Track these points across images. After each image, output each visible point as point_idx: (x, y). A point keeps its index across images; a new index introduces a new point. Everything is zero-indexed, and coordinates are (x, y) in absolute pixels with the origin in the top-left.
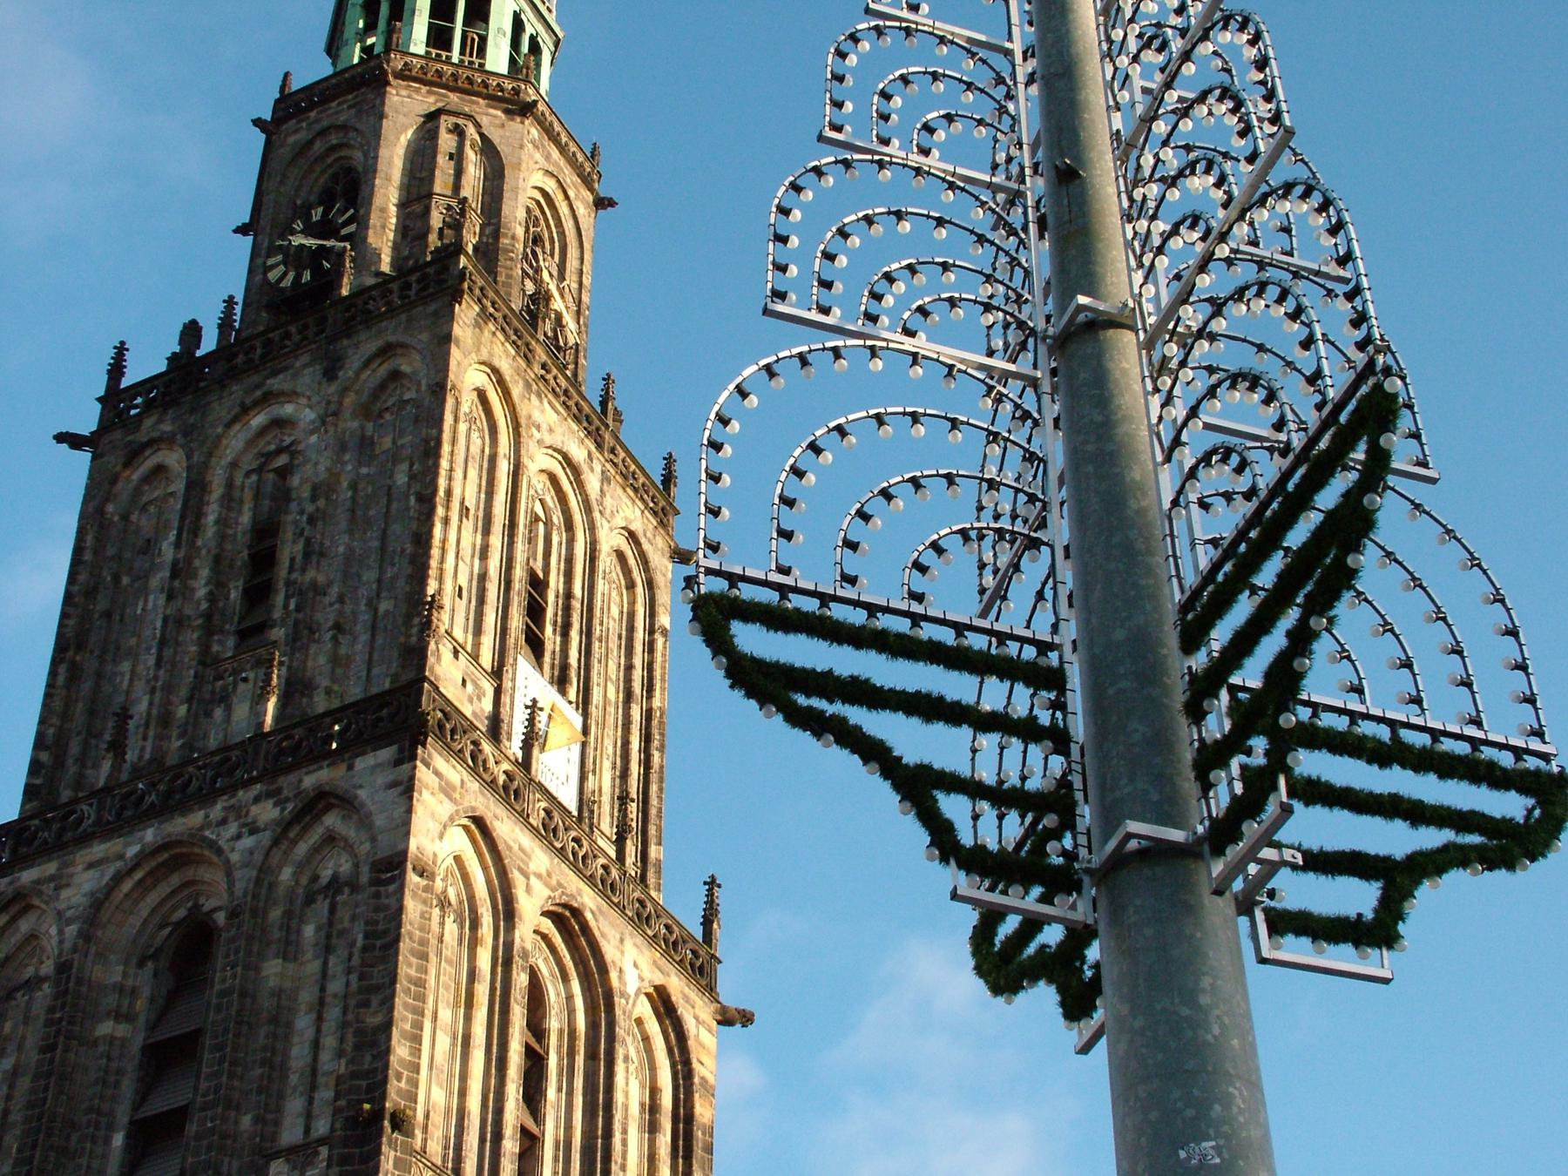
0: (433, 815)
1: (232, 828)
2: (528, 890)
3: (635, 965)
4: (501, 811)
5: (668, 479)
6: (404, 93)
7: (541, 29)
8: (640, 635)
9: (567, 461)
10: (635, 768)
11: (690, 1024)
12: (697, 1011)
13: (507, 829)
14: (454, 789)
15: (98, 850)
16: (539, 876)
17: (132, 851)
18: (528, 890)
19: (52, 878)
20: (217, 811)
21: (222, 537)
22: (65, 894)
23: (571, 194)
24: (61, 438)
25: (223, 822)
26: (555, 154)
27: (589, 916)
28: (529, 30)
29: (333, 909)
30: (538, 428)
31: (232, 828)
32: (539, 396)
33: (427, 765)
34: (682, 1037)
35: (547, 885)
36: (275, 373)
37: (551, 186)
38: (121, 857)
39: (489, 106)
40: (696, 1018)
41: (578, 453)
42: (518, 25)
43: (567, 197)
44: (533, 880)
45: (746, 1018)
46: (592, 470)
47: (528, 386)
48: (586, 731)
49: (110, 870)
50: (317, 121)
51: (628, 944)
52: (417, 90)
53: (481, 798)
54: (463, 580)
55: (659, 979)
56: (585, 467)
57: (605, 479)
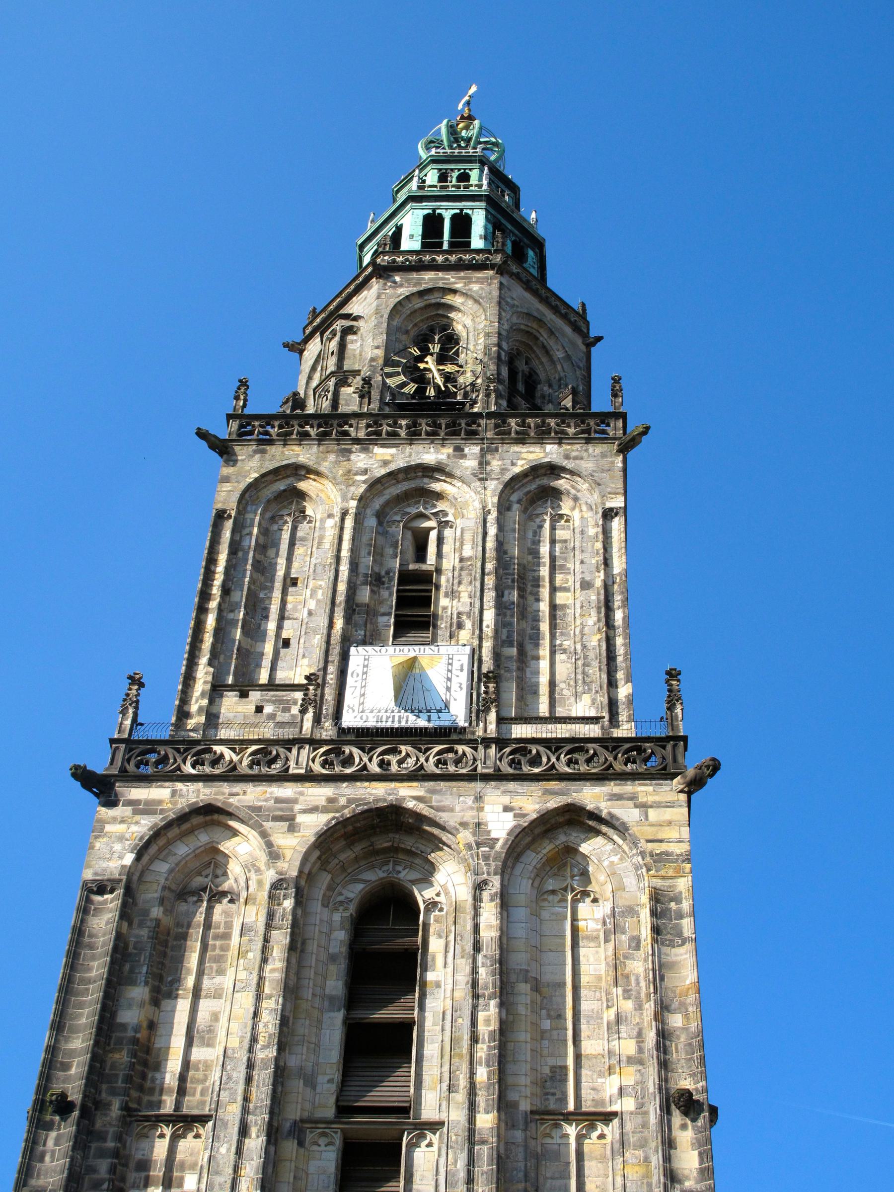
0: (121, 838)
2: (293, 828)
3: (507, 809)
12: (642, 799)
14: (160, 802)
16: (314, 810)
18: (293, 828)
23: (458, 286)
26: (428, 276)
27: (410, 804)
32: (365, 450)
35: (325, 810)
40: (644, 807)
44: (300, 819)
53: (207, 791)
55: (553, 803)
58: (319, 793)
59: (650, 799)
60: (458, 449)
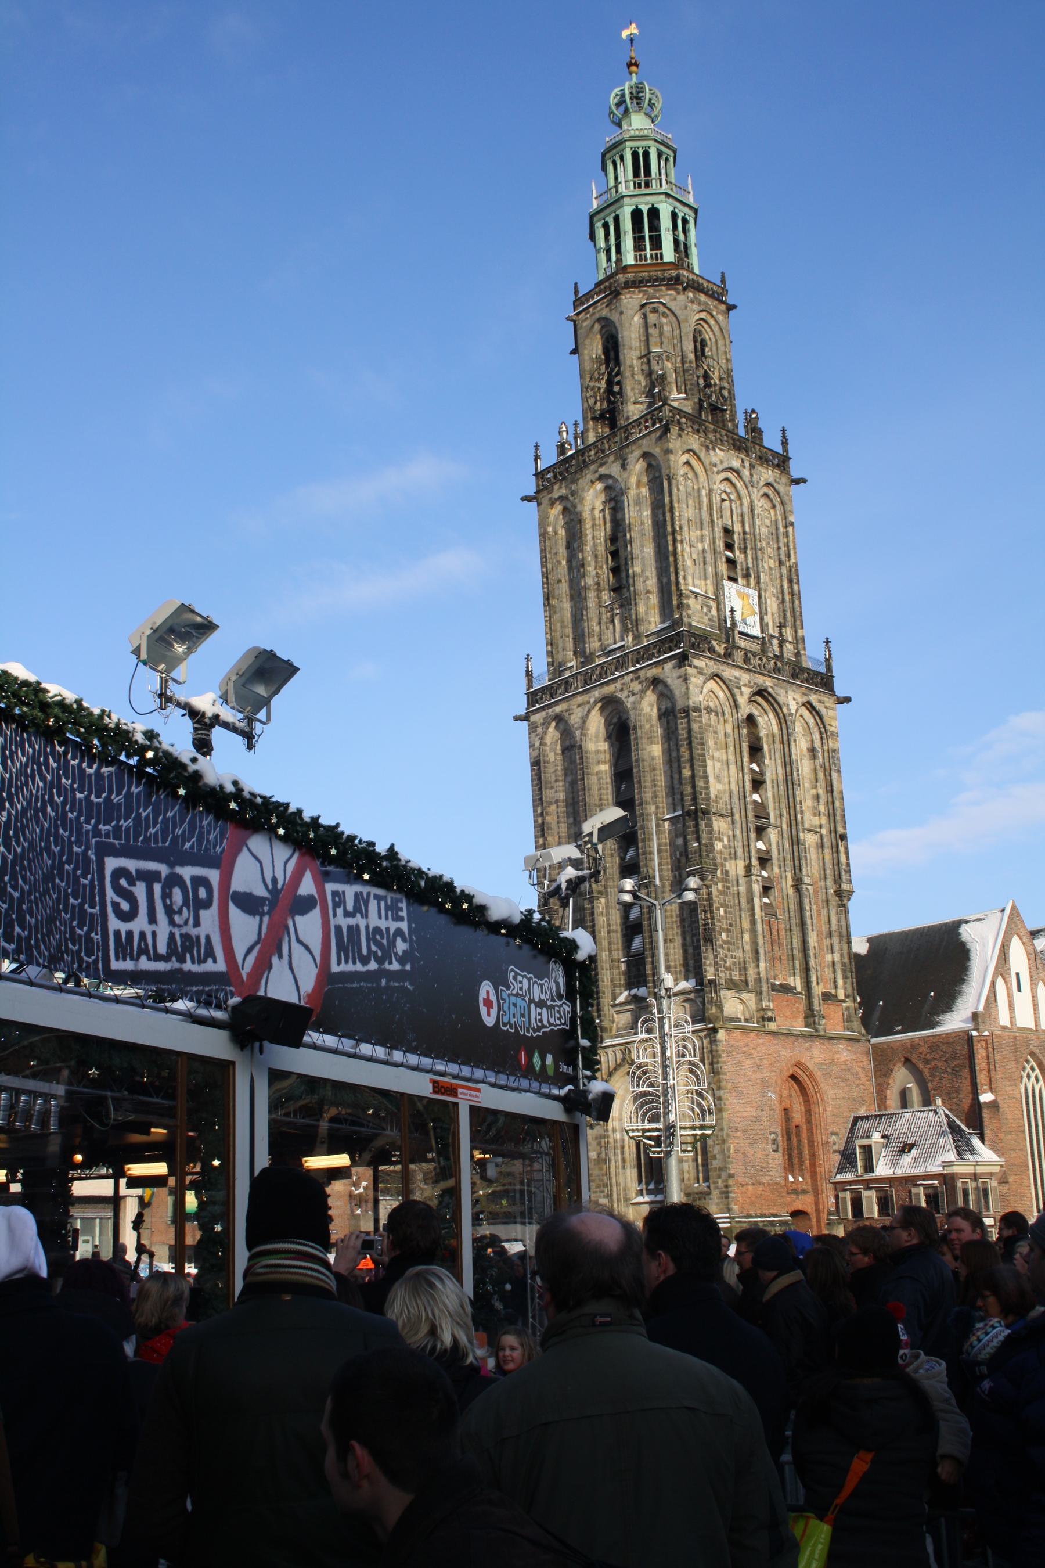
0: (696, 686)
1: (625, 693)
4: (722, 667)
5: (785, 443)
6: (628, 296)
7: (686, 210)
8: (781, 530)
9: (731, 469)
10: (787, 598)
11: (823, 711)
13: (729, 673)
15: (580, 699)
16: (745, 685)
17: (592, 700)
18: (742, 694)
19: (567, 710)
20: (618, 685)
21: (595, 545)
22: (572, 717)
23: (714, 313)
24: (523, 499)
25: (622, 690)
26: (703, 298)
27: (770, 690)
28: (680, 215)
29: (668, 723)
30: (715, 466)
31: (625, 693)
32: (714, 449)
33: (690, 666)
34: (821, 718)
36: (601, 465)
37: (703, 315)
38: (588, 702)
39: (668, 289)
41: (736, 464)
42: (674, 216)
43: (712, 316)
44: (744, 689)
45: (848, 700)
46: (744, 467)
47: (707, 448)
48: (760, 597)
49: (587, 708)
50: (594, 314)
51: (790, 692)
52: (634, 292)
54: (694, 556)
55: (805, 699)
56: (741, 469)
57: (752, 466)
58: (745, 677)
59: (828, 705)
60: (743, 462)
